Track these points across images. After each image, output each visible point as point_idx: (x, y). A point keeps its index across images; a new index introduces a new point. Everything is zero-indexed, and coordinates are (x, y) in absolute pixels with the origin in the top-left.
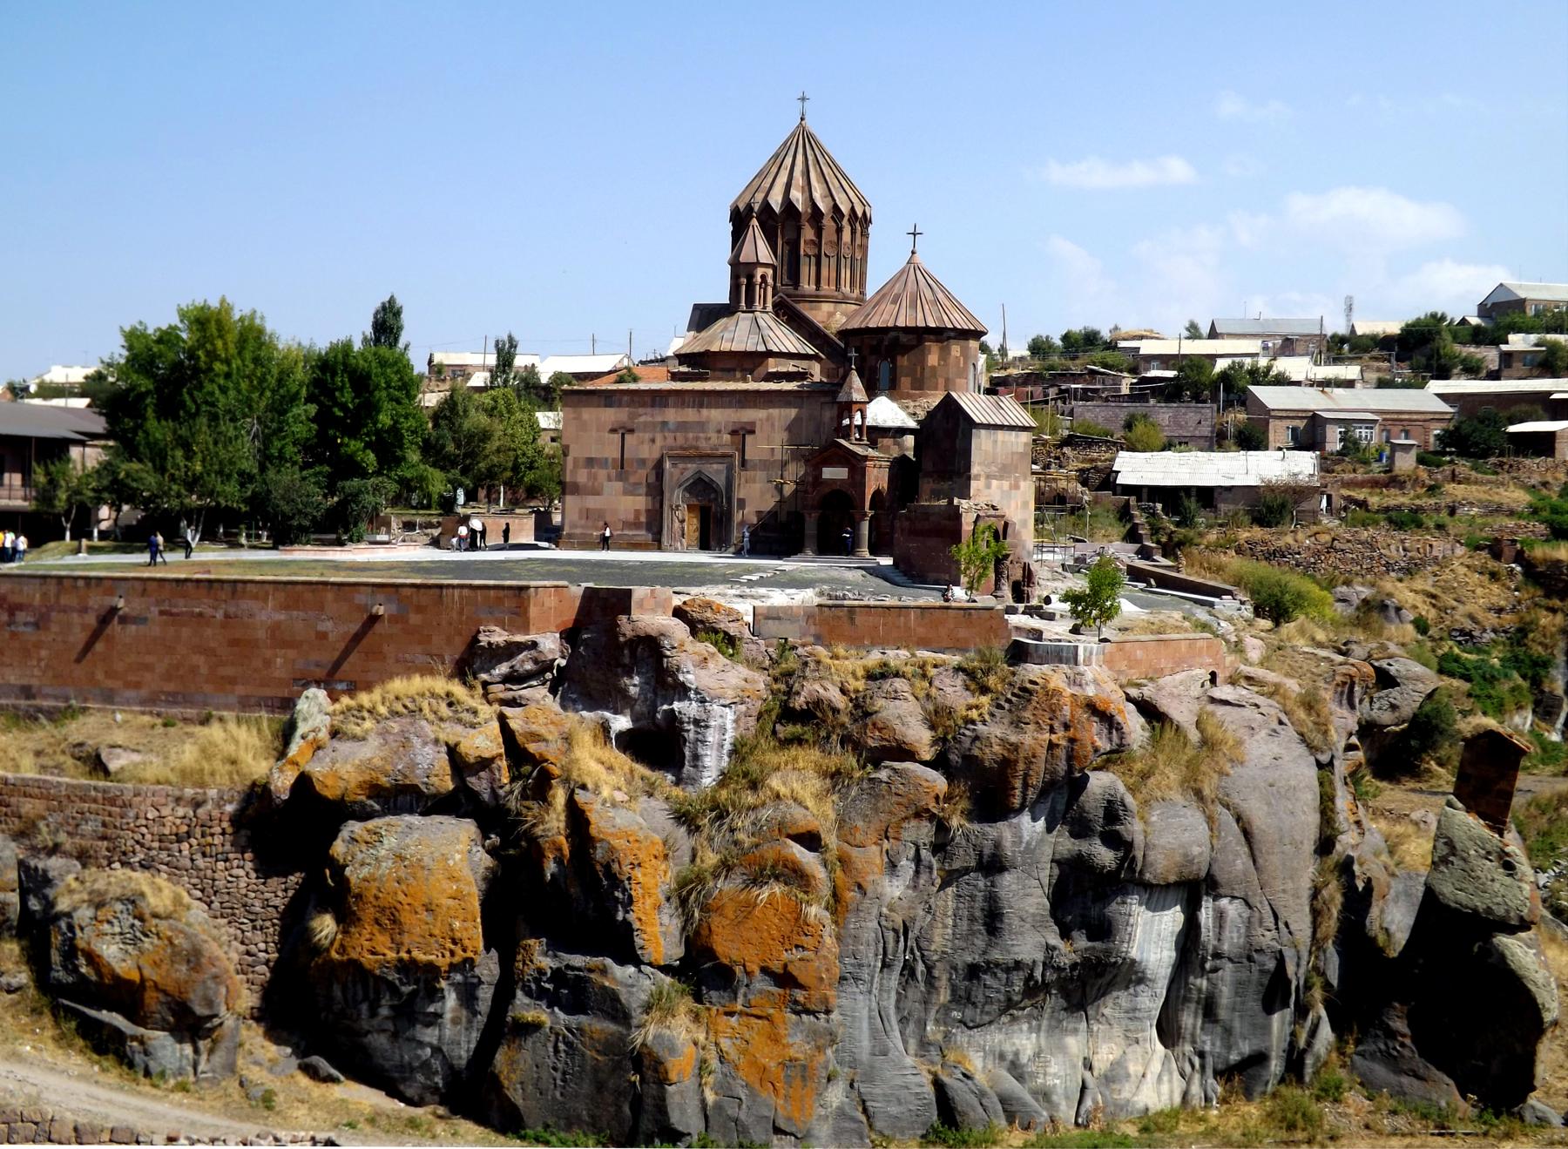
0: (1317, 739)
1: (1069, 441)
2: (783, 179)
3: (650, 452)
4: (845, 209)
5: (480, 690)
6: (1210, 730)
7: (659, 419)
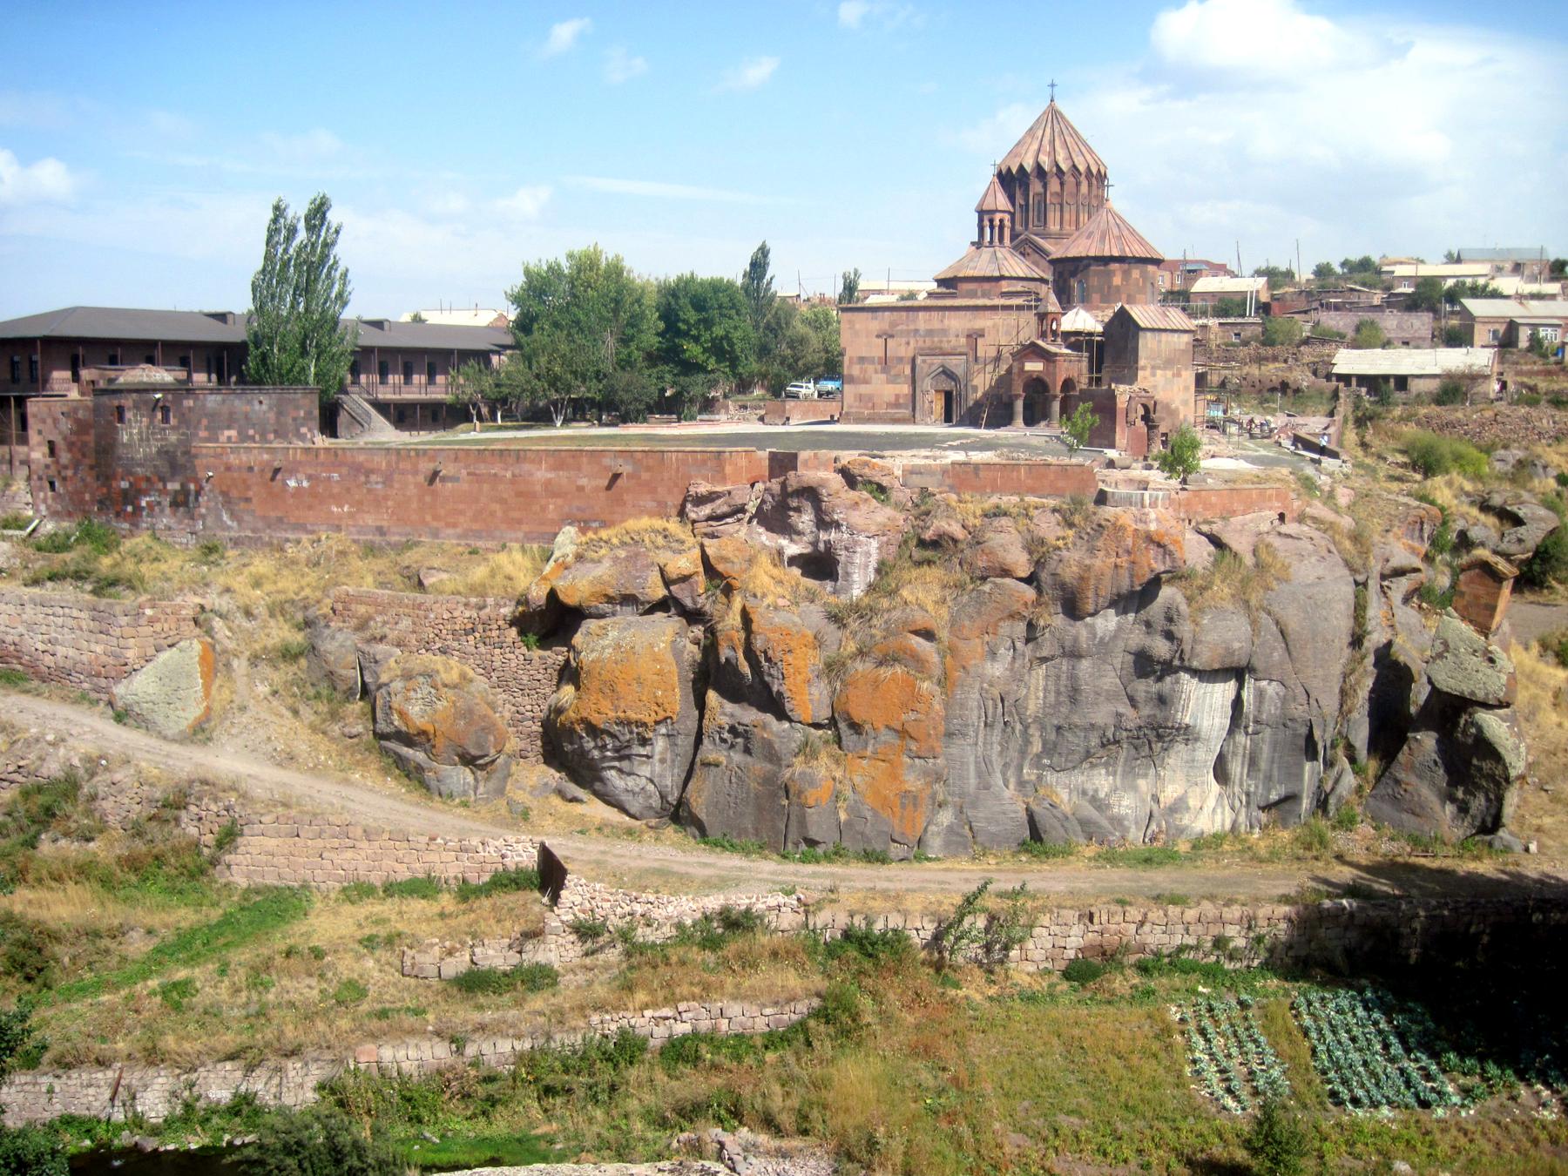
0: (1358, 562)
1: (1306, 342)
2: (1035, 146)
4: (1082, 168)
5: (690, 526)
6: (1264, 555)
7: (912, 327)
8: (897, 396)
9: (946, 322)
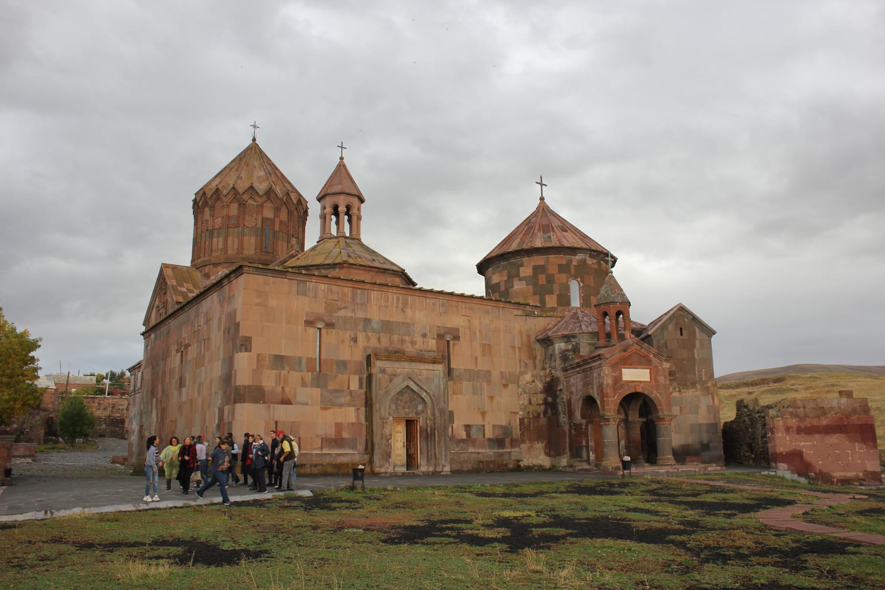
3: (354, 355)
7: (360, 315)
8: (339, 426)
9: (409, 312)
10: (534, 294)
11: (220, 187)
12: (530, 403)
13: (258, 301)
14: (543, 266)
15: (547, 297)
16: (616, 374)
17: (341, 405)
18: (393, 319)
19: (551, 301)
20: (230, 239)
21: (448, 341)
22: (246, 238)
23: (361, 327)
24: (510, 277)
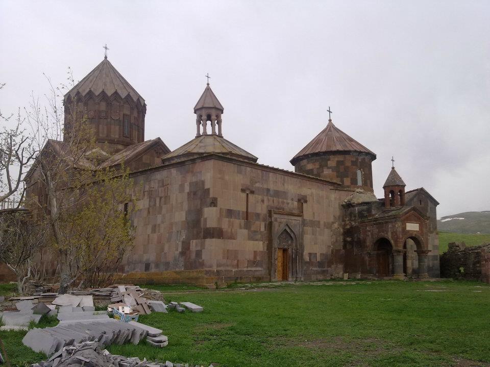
3: (262, 209)
7: (265, 186)
10: (337, 177)
11: (92, 89)
12: (336, 241)
13: (219, 176)
14: (343, 161)
15: (345, 179)
16: (404, 226)
17: (256, 240)
18: (279, 190)
19: (347, 181)
20: (101, 126)
21: (302, 203)
22: (113, 127)
23: (265, 194)
24: (321, 167)
